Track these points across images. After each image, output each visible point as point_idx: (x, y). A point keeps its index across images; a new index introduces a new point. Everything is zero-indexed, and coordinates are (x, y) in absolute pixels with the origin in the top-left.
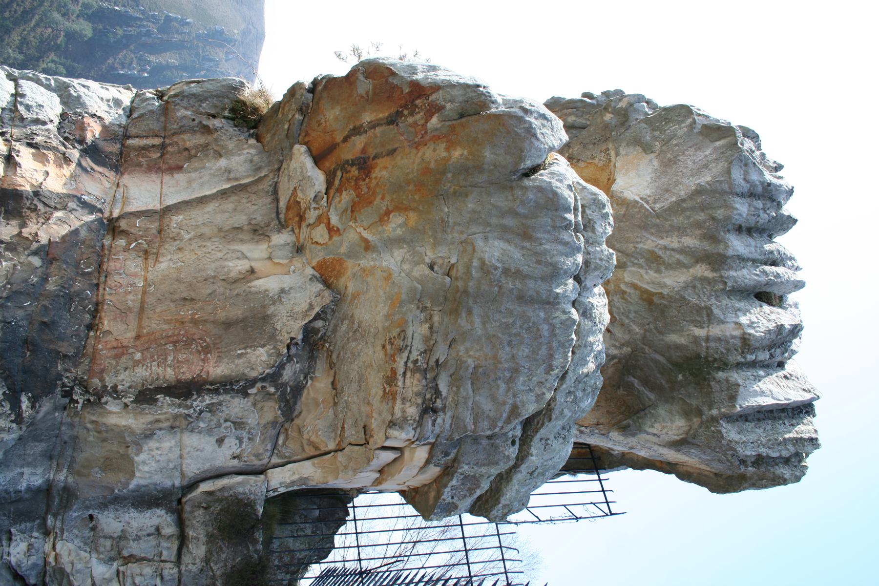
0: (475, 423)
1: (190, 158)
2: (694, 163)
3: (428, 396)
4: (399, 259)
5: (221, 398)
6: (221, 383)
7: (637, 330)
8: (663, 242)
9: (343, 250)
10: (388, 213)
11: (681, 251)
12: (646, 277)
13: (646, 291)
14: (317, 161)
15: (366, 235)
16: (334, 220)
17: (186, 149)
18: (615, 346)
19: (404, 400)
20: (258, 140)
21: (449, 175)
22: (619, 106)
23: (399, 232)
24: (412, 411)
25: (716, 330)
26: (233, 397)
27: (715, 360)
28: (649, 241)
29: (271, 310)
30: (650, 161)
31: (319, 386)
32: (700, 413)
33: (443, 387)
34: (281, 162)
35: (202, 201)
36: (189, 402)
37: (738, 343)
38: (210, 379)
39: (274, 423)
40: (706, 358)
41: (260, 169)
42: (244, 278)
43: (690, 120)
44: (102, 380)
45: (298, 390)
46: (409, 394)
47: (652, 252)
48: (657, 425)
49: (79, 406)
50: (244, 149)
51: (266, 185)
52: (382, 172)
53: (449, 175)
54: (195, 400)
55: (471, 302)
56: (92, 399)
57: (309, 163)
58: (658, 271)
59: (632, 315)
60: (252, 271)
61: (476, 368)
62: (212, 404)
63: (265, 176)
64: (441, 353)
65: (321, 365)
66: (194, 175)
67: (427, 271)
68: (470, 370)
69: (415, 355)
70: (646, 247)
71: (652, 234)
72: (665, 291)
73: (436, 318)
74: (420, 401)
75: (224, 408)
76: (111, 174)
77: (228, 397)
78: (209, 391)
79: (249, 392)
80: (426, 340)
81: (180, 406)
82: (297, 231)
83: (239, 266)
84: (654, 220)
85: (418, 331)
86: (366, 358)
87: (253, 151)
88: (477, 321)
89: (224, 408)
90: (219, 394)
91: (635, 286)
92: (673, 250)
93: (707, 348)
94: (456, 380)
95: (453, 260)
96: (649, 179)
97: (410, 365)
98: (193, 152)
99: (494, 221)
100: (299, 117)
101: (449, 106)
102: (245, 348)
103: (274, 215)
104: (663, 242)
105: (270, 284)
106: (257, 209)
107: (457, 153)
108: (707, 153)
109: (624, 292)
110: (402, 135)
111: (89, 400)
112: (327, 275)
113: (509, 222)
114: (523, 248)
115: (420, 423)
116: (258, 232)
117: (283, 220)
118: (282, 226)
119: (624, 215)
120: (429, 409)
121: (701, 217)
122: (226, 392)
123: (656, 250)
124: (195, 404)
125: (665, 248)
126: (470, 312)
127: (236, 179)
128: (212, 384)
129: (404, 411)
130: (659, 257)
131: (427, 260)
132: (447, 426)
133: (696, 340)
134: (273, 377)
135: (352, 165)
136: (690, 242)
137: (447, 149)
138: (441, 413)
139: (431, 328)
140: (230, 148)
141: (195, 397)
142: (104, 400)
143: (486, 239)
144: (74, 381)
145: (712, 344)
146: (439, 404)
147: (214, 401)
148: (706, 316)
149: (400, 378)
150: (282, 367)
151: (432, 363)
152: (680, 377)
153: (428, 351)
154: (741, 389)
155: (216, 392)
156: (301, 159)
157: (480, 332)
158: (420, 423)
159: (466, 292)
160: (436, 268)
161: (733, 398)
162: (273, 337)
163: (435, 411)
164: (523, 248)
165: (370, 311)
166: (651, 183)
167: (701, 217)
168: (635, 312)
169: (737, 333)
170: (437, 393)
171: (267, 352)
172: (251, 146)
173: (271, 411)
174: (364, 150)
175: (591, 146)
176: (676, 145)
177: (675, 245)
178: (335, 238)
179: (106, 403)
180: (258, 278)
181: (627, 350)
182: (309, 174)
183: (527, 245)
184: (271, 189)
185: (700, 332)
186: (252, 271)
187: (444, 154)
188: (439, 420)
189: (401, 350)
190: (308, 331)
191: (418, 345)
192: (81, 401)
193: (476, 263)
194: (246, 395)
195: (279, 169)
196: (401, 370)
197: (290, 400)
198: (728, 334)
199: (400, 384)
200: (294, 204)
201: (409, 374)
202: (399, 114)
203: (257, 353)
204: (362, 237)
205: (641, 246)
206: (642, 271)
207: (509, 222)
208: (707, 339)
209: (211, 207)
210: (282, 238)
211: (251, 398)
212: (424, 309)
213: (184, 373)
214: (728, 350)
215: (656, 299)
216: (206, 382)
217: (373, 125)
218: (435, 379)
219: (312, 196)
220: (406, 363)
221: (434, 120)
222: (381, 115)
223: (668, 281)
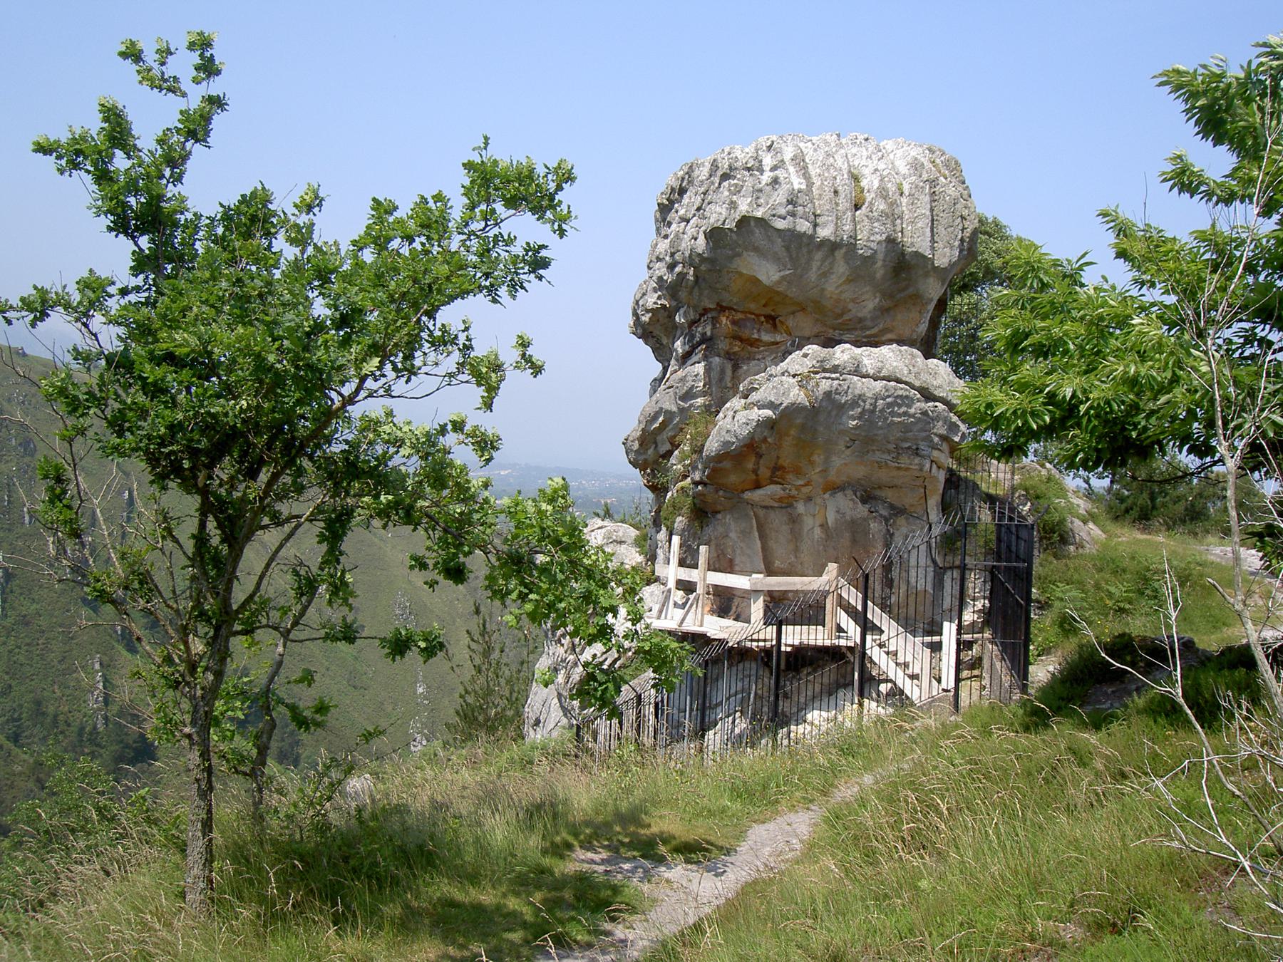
1: (724, 555)
9: (821, 480)
11: (823, 261)
14: (758, 486)
16: (801, 482)
24: (917, 460)
25: (880, 256)
29: (848, 518)
31: (890, 495)
33: (907, 445)
35: (765, 549)
39: (907, 519)
45: (892, 507)
51: (761, 513)
52: (785, 462)
57: (760, 492)
60: (821, 526)
64: (891, 447)
65: (878, 493)
66: (738, 552)
76: (736, 601)
83: (818, 531)
85: (879, 456)
86: (883, 475)
91: (837, 287)
94: (905, 440)
100: (721, 493)
105: (831, 518)
106: (777, 520)
107: (792, 432)
112: (834, 488)
113: (834, 413)
115: (922, 457)
116: (795, 520)
118: (790, 505)
120: (917, 452)
121: (805, 250)
133: (883, 266)
134: (887, 520)
136: (818, 256)
148: (869, 260)
150: (881, 515)
153: (889, 452)
156: (757, 496)
158: (922, 457)
162: (865, 519)
165: (859, 472)
167: (805, 250)
170: (909, 448)
173: (901, 521)
185: (880, 263)
186: (821, 526)
190: (864, 501)
191: (886, 456)
197: (898, 511)
200: (780, 500)
202: (757, 453)
207: (834, 413)
209: (771, 544)
210: (801, 508)
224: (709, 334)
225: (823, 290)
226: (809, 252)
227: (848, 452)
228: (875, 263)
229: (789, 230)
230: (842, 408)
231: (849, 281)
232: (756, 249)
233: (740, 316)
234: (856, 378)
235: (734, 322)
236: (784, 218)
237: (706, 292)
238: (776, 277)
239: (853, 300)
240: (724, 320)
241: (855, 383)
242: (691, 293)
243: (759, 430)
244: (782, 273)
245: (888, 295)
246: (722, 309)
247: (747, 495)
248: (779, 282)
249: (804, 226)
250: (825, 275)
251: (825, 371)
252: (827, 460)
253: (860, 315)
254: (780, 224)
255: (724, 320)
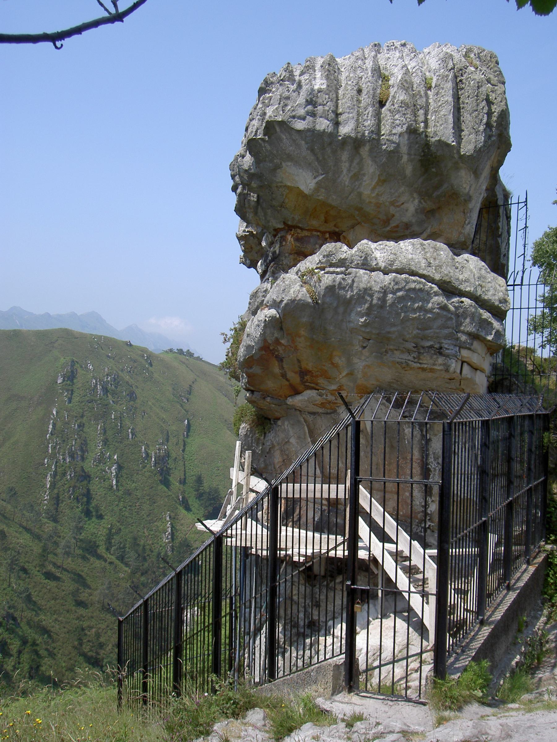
0: (448, 328)
2: (291, 146)
3: (433, 352)
4: (358, 361)
5: (431, 453)
6: (423, 453)
7: (403, 189)
8: (345, 172)
9: (352, 385)
10: (333, 364)
11: (351, 161)
12: (367, 182)
13: (377, 183)
14: (297, 392)
15: (344, 374)
17: (284, 461)
18: (412, 201)
19: (434, 365)
20: (278, 419)
21: (314, 336)
22: (246, 178)
23: (343, 359)
24: (441, 360)
25: (404, 149)
26: (431, 447)
27: (423, 151)
28: (344, 179)
30: (287, 166)
32: (456, 163)
33: (428, 344)
34: (296, 409)
36: (432, 470)
37: (413, 136)
38: (421, 458)
40: (421, 156)
41: (299, 421)
42: (366, 436)
43: (260, 141)
44: (419, 513)
46: (431, 362)
47: (352, 178)
48: (464, 186)
49: (433, 524)
50: (285, 428)
51: (310, 418)
52: (309, 365)
53: (314, 336)
54: (431, 466)
55: (384, 332)
56: (428, 518)
57: (299, 398)
58: (364, 175)
59: (393, 191)
61: (418, 329)
62: (434, 457)
63: (304, 418)
64: (410, 345)
67: (366, 350)
68: (419, 332)
69: (410, 358)
70: (348, 180)
71: (339, 177)
72: (378, 173)
73: (391, 347)
74: (435, 357)
75: (437, 451)
77: (431, 449)
78: (426, 460)
79: (428, 438)
80: (403, 352)
81: (434, 474)
82: (339, 405)
84: (330, 175)
87: (286, 423)
88: (393, 329)
89: (437, 451)
90: (429, 454)
91: (373, 189)
92: (350, 166)
93: (415, 155)
94: (424, 338)
95: (361, 338)
96: (301, 171)
97: (416, 360)
98: (285, 457)
99: (340, 318)
100: (268, 399)
101: (276, 335)
102: (405, 439)
103: (329, 416)
104: (345, 172)
107: (302, 332)
108: (285, 137)
109: (378, 195)
110: (289, 356)
111: (429, 520)
114: (355, 304)
115: (447, 356)
117: (332, 411)
119: (326, 189)
120: (440, 351)
121: (329, 150)
122: (427, 450)
123: (350, 175)
124: (433, 467)
125: (349, 170)
126: (389, 333)
127: (305, 434)
128: (423, 457)
129: (440, 365)
130: (355, 174)
131: (360, 349)
132: (449, 342)
135: (303, 378)
136: (345, 156)
137: (300, 337)
138: (442, 345)
139: (396, 350)
140: (284, 436)
141: (430, 466)
142: (430, 513)
143: (349, 322)
144: (419, 526)
145: (412, 152)
146: (437, 346)
147: (432, 457)
148: (394, 154)
149: (422, 366)
151: (415, 350)
152: (434, 170)
153: (409, 352)
154: (443, 139)
155: (427, 455)
156: (297, 401)
157: (399, 328)
158: (447, 356)
159: (378, 334)
160: (365, 345)
161: (448, 145)
163: (441, 348)
164: (355, 304)
165: (386, 375)
166: (303, 170)
167: (329, 150)
168: (391, 189)
169: (406, 137)
170: (431, 347)
171: (407, 428)
172: (283, 424)
174: (296, 373)
175: (274, 196)
176: (277, 151)
177: (347, 165)
178: (345, 388)
179: (431, 511)
180: (366, 429)
181: (415, 195)
182: (306, 398)
183: (354, 302)
184: (312, 416)
185: (405, 158)
187: (303, 338)
188: (446, 346)
189: (408, 365)
191: (406, 356)
192: (429, 523)
193: (363, 329)
194: (430, 440)
195: (300, 411)
196: (418, 365)
198: (406, 142)
199: (426, 366)
200: (322, 405)
201: (421, 361)
202: (277, 357)
203: (407, 433)
204: (345, 376)
205: (347, 183)
206: (364, 183)
207: (341, 310)
208: (409, 154)
211: (432, 437)
212: (386, 352)
213: (417, 471)
214: (417, 143)
215: (382, 178)
216: (422, 461)
217: (282, 368)
218: (423, 348)
219: (319, 397)
220: (415, 362)
221: (283, 342)
222: (277, 364)
223: (371, 170)
224: (277, 252)
225: (360, 194)
226: (334, 152)
227: (366, 352)
228: (400, 158)
229: (308, 130)
230: (348, 304)
231: (382, 182)
232: (289, 158)
233: (306, 233)
234: (362, 271)
235: (297, 239)
236: (304, 119)
237: (269, 212)
238: (312, 184)
239: (392, 203)
240: (289, 237)
241: (360, 277)
242: (256, 213)
243: (268, 331)
244: (317, 179)
245: (424, 195)
246: (289, 228)
247: (290, 401)
248: (318, 188)
249: (323, 124)
250: (357, 177)
251: (331, 265)
252: (349, 362)
253: (405, 220)
254: (300, 125)
255: (289, 237)
